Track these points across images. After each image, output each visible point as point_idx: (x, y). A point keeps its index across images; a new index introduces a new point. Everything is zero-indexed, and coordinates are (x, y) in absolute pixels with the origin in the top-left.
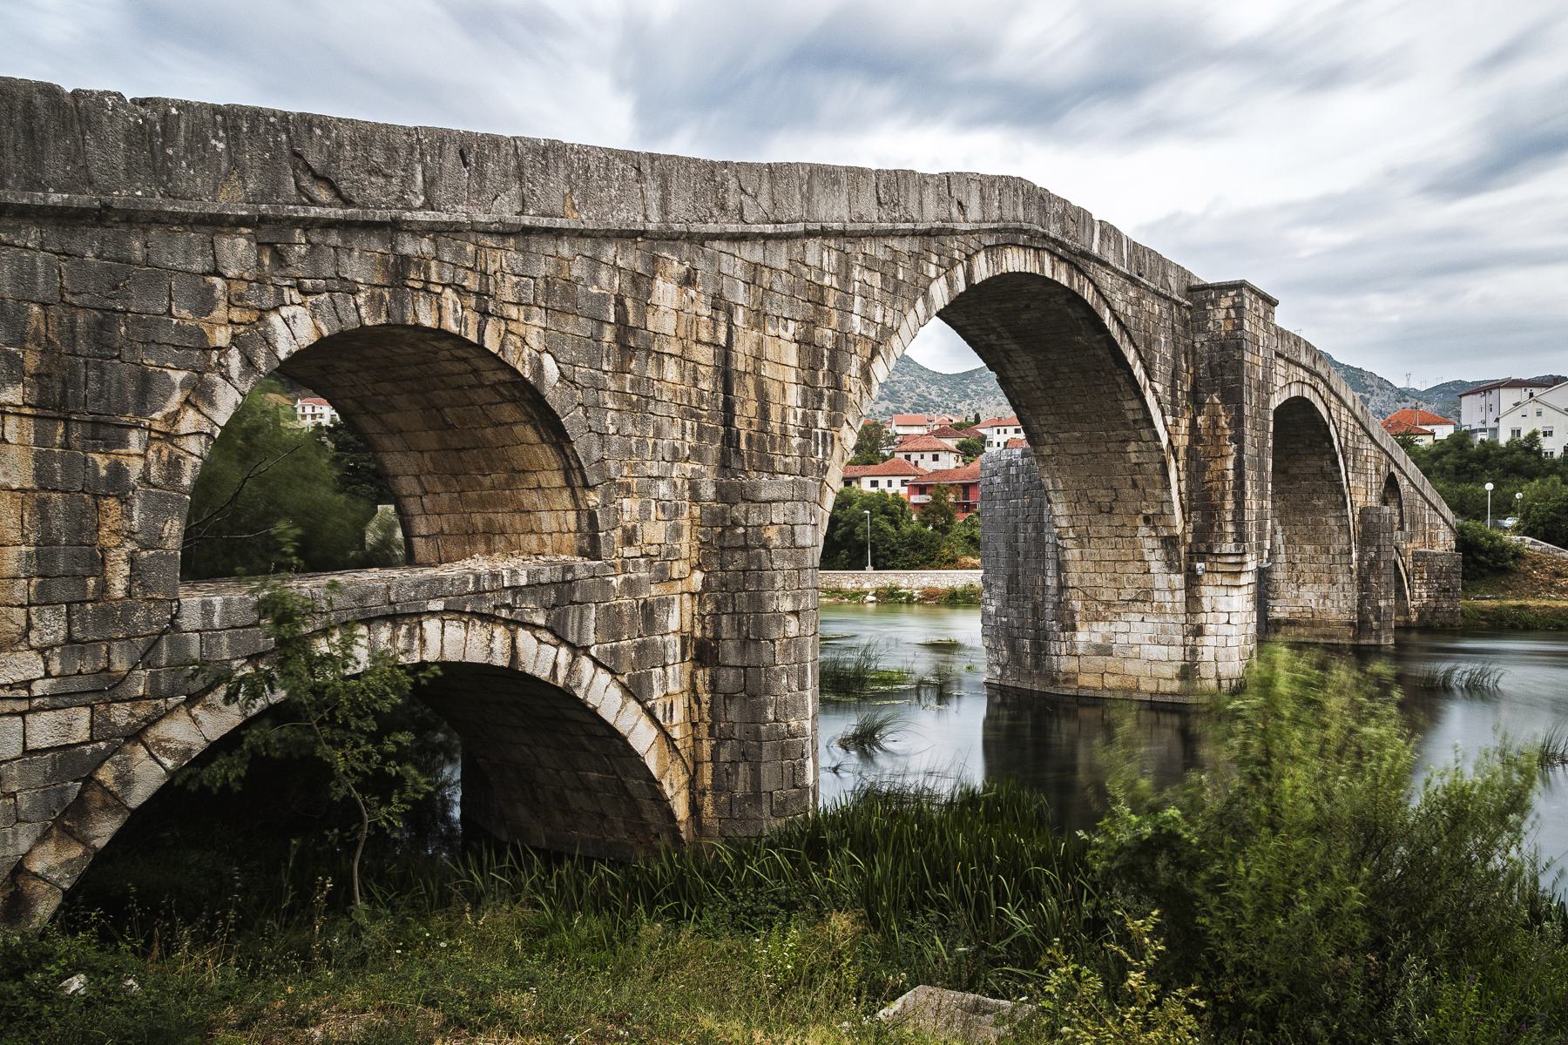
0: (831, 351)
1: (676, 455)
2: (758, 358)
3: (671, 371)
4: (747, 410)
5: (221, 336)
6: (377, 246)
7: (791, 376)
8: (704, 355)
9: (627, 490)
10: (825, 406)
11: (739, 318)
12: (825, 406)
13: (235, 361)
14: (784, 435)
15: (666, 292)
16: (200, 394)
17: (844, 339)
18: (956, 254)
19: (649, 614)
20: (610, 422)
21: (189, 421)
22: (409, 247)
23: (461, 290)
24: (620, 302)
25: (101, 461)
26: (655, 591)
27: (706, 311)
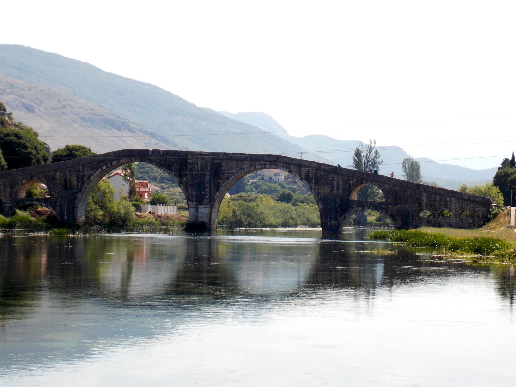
0: (82, 177)
1: (59, 188)
2: (70, 178)
3: (58, 181)
4: (68, 184)
5: (19, 182)
6: (30, 175)
7: (75, 180)
8: (62, 179)
9: (53, 191)
10: (80, 182)
11: (67, 175)
12: (80, 182)
13: (20, 184)
14: (74, 186)
15: (58, 174)
16: (18, 186)
17: (84, 176)
18: (107, 162)
19: (55, 202)
20: (51, 186)
21: (17, 188)
22: (32, 175)
23: (37, 177)
24: (52, 176)
25: (13, 190)
26: (56, 200)
27: (63, 175)
